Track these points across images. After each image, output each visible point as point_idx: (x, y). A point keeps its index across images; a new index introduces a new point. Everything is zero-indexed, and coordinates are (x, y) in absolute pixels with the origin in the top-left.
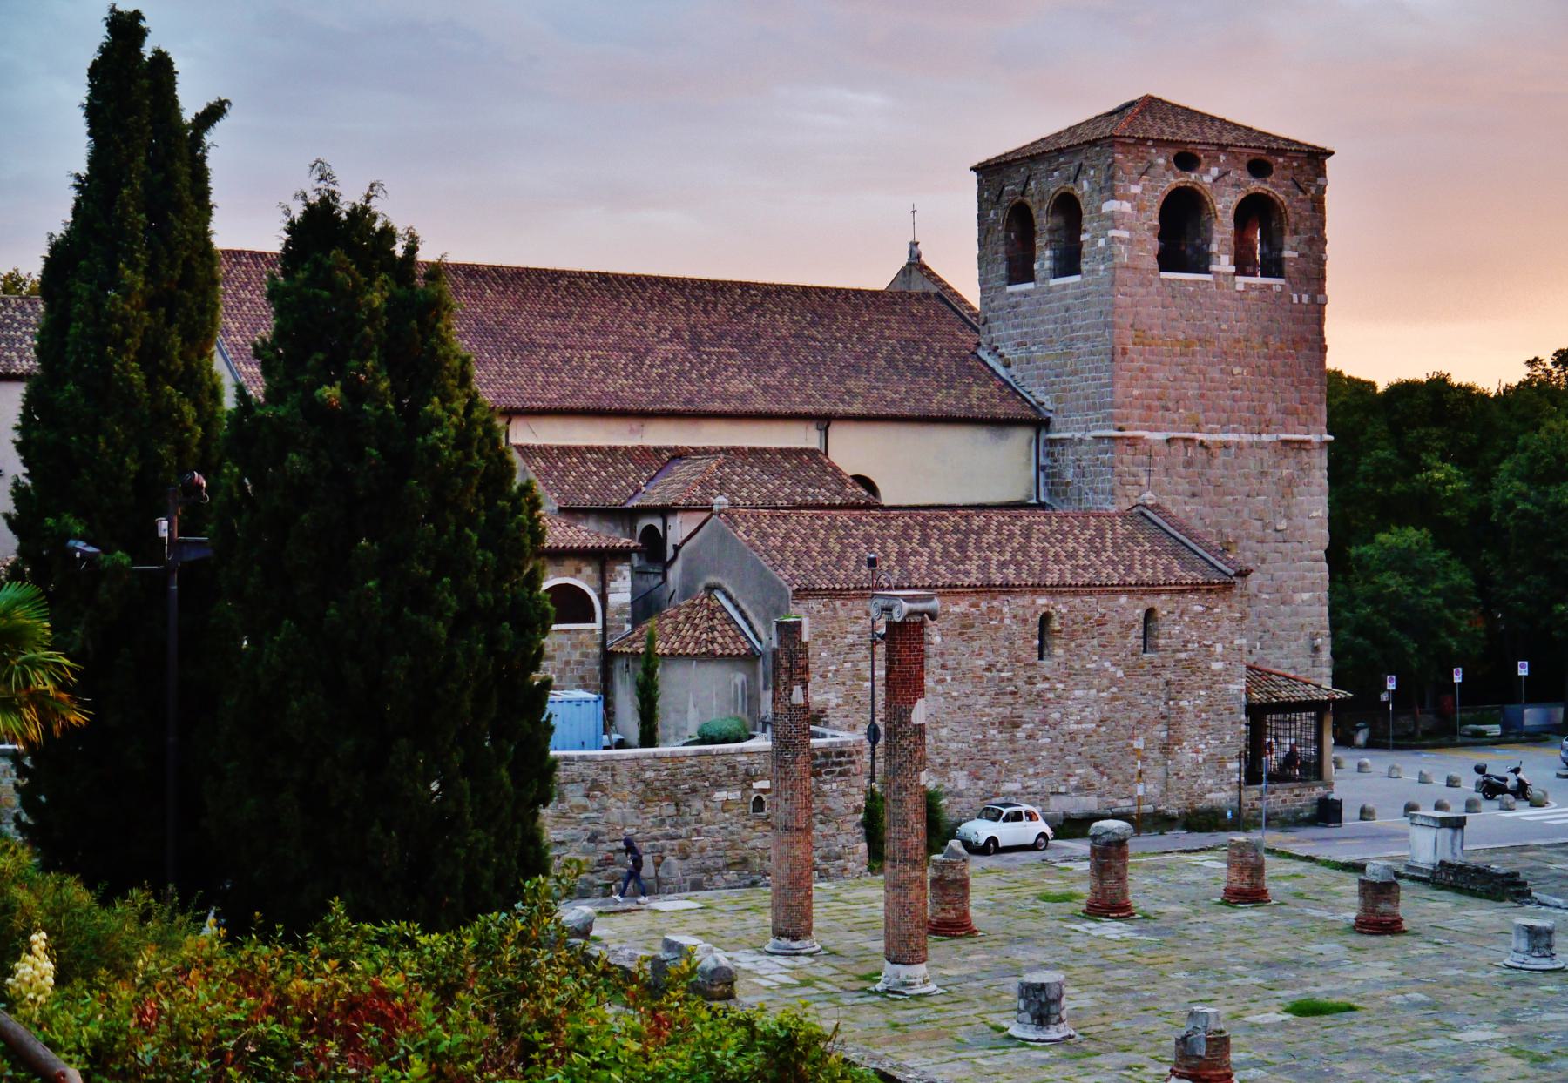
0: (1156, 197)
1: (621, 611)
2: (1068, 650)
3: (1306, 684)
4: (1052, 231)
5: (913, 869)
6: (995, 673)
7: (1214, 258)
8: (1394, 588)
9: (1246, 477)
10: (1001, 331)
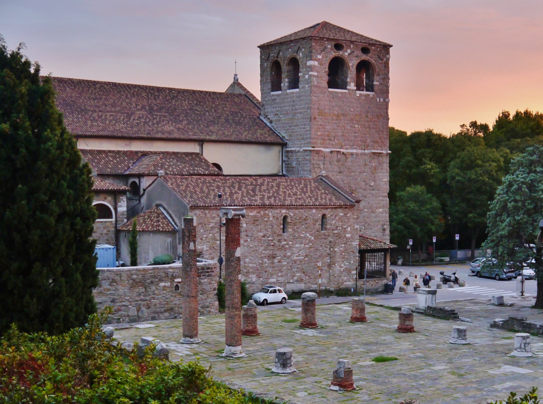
0: (327, 60)
1: (123, 214)
2: (294, 230)
3: (381, 242)
4: (288, 72)
5: (236, 311)
6: (266, 238)
7: (349, 84)
8: (412, 207)
9: (359, 166)
10: (269, 109)
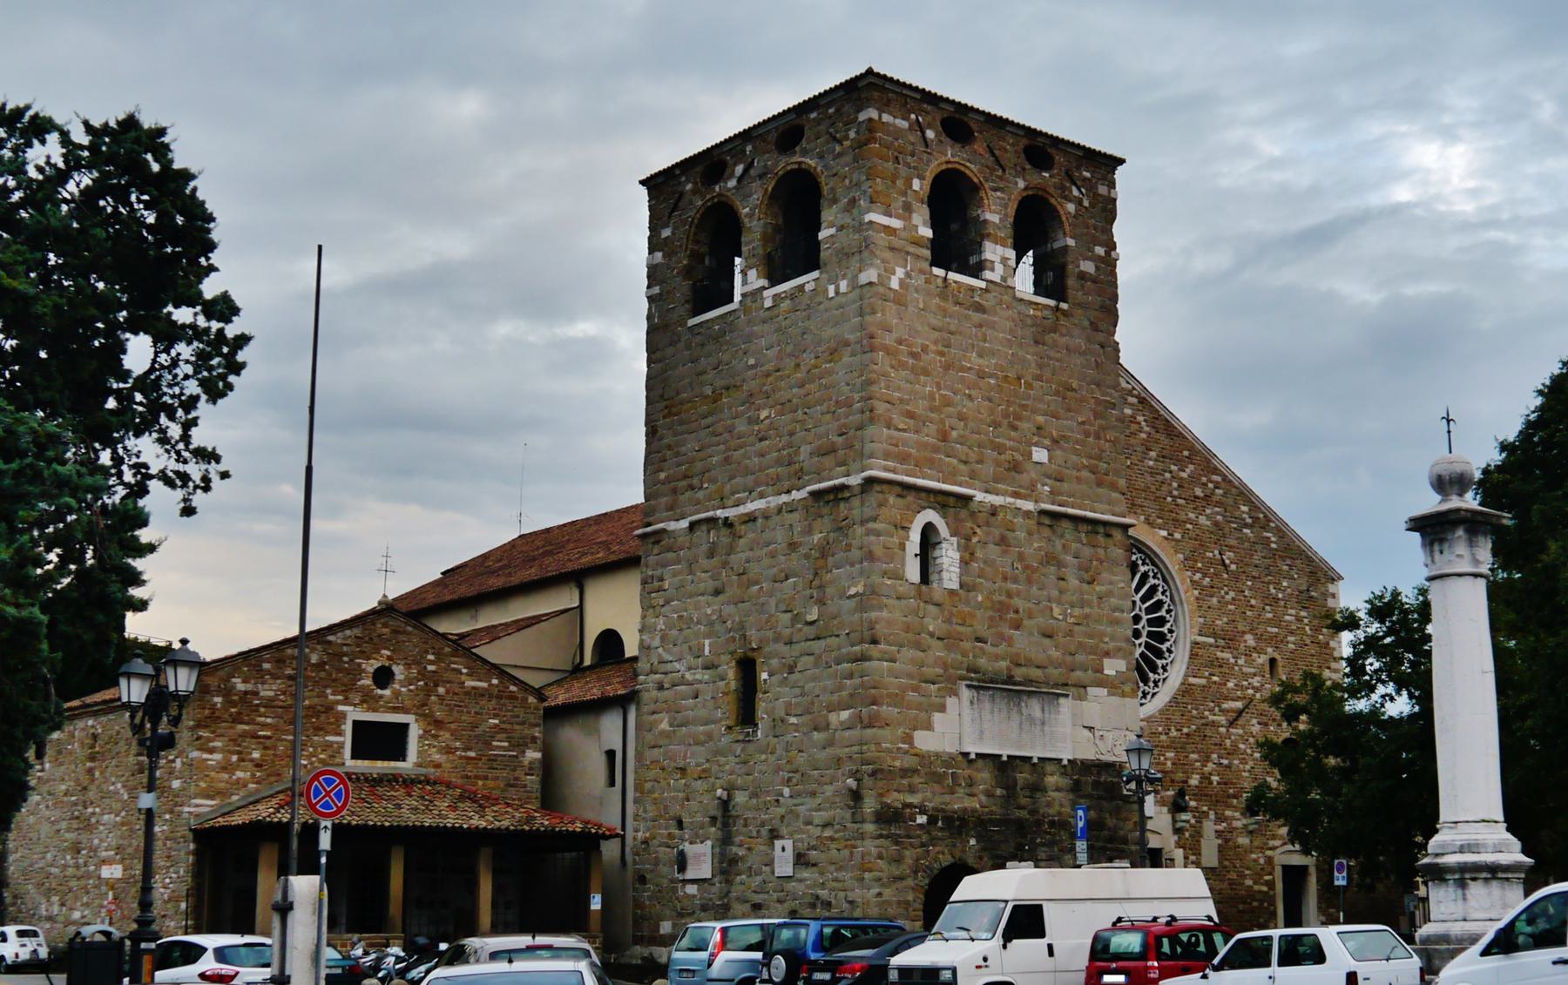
9: (773, 555)
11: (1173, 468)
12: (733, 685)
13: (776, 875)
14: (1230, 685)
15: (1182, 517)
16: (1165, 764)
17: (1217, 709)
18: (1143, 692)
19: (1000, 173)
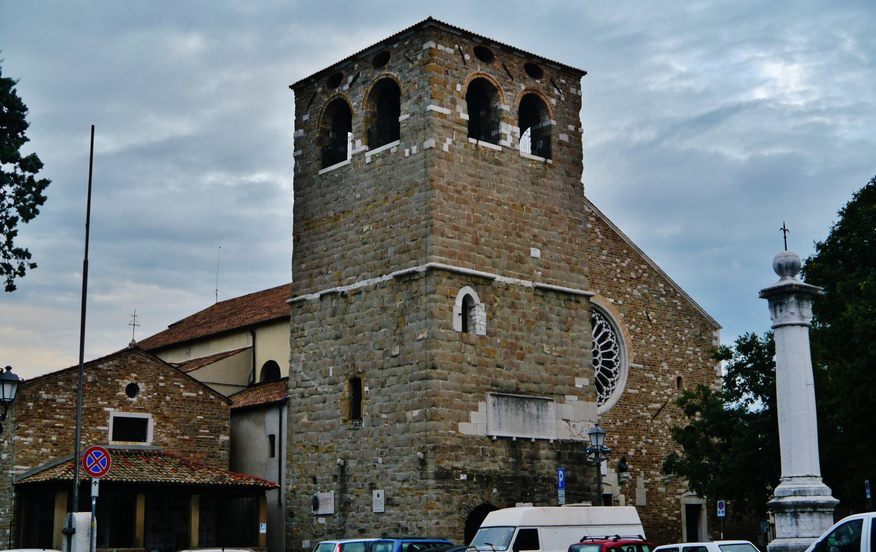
11: (618, 260)
12: (347, 395)
13: (374, 511)
14: (653, 393)
15: (623, 290)
16: (613, 442)
17: (645, 408)
18: (600, 398)
19: (510, 80)
